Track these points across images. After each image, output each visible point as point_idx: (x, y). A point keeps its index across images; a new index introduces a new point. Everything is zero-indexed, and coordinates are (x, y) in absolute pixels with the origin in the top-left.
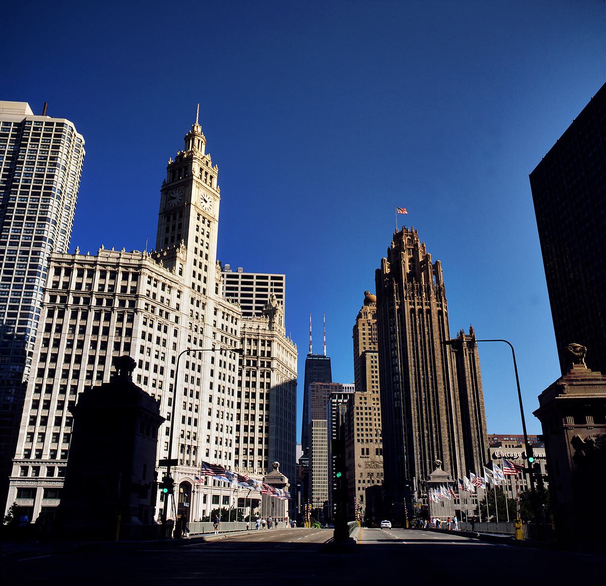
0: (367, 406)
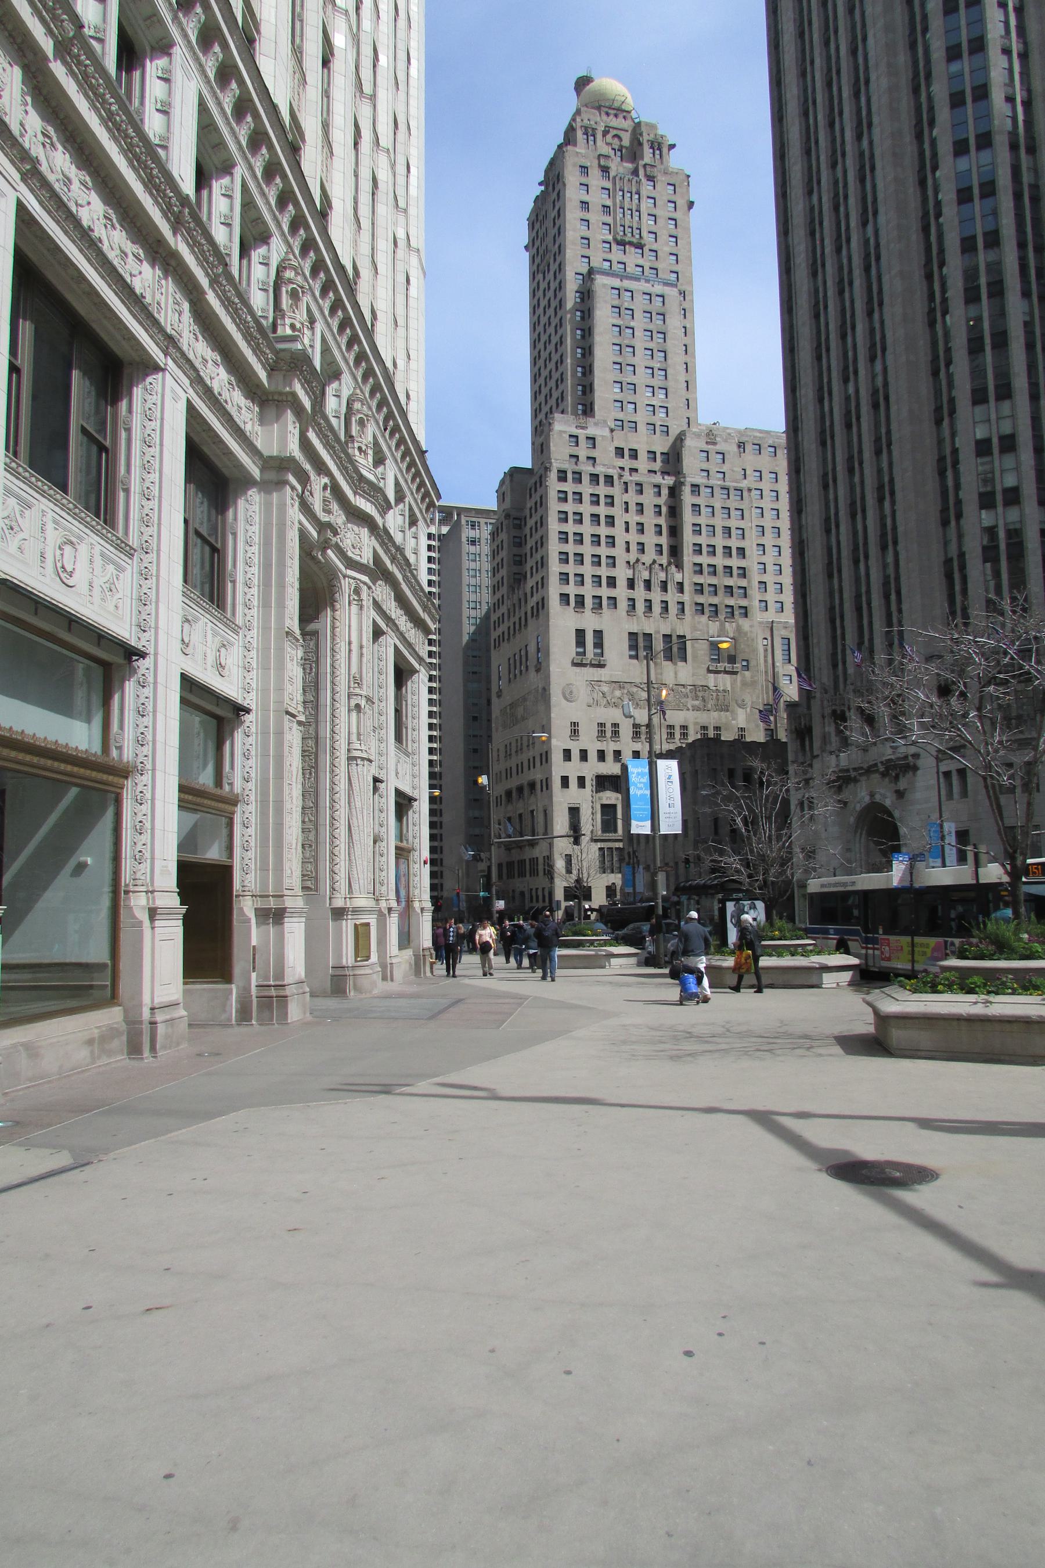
0: (599, 470)
